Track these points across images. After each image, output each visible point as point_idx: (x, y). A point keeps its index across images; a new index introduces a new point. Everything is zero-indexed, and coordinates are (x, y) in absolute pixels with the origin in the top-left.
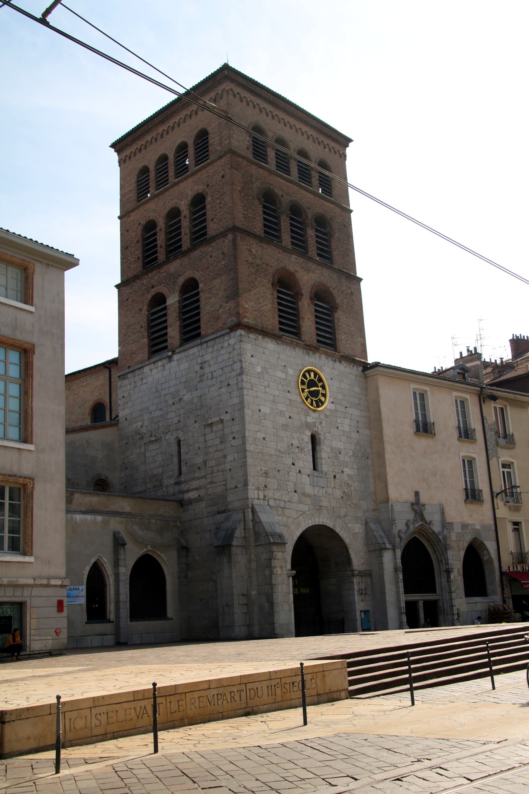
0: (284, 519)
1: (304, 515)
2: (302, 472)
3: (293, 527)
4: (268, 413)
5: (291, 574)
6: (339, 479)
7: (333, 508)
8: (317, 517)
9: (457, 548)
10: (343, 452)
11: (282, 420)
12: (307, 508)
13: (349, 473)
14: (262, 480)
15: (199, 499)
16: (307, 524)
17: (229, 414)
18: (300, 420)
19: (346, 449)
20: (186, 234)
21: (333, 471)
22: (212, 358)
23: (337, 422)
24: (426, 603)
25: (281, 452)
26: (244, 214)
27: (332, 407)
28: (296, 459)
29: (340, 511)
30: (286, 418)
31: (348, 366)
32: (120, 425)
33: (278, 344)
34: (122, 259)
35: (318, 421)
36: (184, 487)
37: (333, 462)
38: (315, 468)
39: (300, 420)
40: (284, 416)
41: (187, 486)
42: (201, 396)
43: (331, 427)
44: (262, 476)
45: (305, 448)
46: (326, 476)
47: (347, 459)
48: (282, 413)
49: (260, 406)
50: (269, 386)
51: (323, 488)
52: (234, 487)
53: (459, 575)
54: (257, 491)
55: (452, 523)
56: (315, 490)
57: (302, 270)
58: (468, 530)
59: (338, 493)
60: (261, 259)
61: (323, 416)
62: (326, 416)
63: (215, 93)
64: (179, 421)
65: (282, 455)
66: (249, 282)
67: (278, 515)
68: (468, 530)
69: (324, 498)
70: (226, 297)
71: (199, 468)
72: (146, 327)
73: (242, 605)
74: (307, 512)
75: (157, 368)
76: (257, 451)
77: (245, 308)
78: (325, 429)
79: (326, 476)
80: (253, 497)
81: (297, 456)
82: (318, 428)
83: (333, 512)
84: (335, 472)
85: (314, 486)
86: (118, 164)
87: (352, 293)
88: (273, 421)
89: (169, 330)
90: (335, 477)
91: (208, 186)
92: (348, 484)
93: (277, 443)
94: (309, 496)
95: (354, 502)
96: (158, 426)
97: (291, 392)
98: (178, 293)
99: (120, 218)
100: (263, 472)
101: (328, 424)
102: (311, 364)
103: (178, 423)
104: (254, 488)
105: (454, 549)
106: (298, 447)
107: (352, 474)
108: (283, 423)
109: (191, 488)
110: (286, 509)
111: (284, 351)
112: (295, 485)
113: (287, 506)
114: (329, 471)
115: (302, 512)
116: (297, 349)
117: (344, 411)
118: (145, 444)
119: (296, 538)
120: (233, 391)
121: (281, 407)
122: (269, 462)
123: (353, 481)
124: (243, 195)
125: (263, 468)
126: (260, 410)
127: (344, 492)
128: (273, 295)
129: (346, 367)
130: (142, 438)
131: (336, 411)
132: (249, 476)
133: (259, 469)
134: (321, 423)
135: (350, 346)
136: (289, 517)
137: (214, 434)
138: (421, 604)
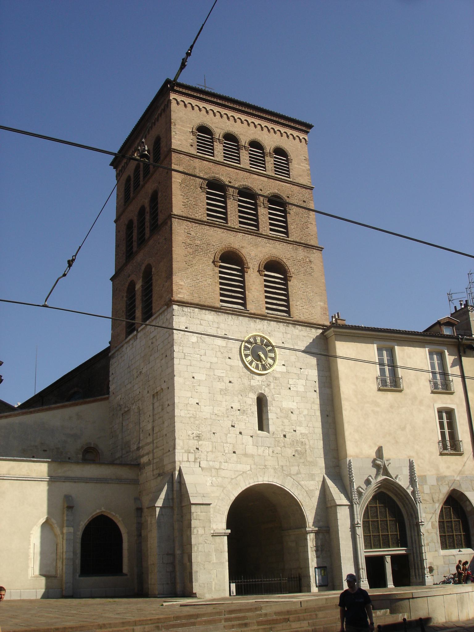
0: (218, 480)
1: (245, 475)
2: (242, 433)
4: (204, 379)
5: (225, 533)
6: (290, 439)
7: (282, 466)
8: (261, 476)
10: (296, 412)
11: (220, 386)
12: (248, 467)
13: (303, 432)
14: (193, 444)
15: (149, 463)
16: (247, 483)
17: (166, 383)
18: (242, 384)
19: (299, 409)
20: (147, 227)
21: (282, 431)
22: (158, 333)
23: (289, 384)
24: (393, 557)
26: (183, 202)
27: (284, 369)
28: (237, 421)
29: (290, 469)
30: (225, 383)
31: (303, 329)
32: (111, 399)
33: (218, 314)
34: (116, 255)
35: (265, 383)
36: (142, 452)
37: (283, 422)
38: (261, 428)
39: (242, 384)
40: (223, 381)
41: (143, 451)
42: (151, 368)
43: (282, 389)
44: (194, 440)
45: (247, 411)
46: (274, 436)
48: (220, 379)
49: (193, 374)
50: (205, 354)
51: (269, 447)
52: (168, 451)
53: (432, 528)
54: (187, 454)
55: (425, 476)
56: (259, 451)
57: (250, 246)
58: (445, 482)
59: (290, 452)
60: (201, 240)
61: (272, 378)
62: (276, 378)
63: (164, 105)
64: (140, 392)
65: (219, 418)
66: (185, 261)
67: (211, 476)
68: (445, 482)
69: (270, 458)
70: (166, 277)
71: (149, 435)
72: (125, 311)
73: (167, 564)
74: (248, 472)
75: (129, 346)
76: (188, 416)
77: (180, 285)
78: (273, 391)
79: (274, 436)
80: (181, 460)
81: (237, 419)
82: (265, 390)
83: (282, 471)
84: (285, 432)
85: (257, 446)
86: (116, 178)
87: (310, 261)
88: (208, 387)
89: (137, 311)
90: (285, 436)
91: (159, 183)
92: (302, 442)
93: (214, 407)
94: (252, 456)
96: (129, 398)
97: (231, 358)
98: (141, 278)
99: (116, 221)
100: (194, 435)
101: (277, 386)
102: (258, 331)
103: (139, 394)
104: (183, 451)
105: (428, 501)
106: (239, 410)
107: (307, 432)
108: (221, 388)
109: (145, 453)
110: (221, 470)
111: (225, 321)
112: (234, 446)
113: (223, 467)
114: (277, 431)
115: (242, 472)
117: (299, 373)
118: (122, 414)
119: (233, 498)
120: (169, 362)
121: (218, 373)
122: (203, 425)
123: (308, 439)
124: (184, 185)
125: (195, 432)
126: (193, 378)
127: (296, 451)
128: (214, 270)
129: (302, 330)
130: (120, 410)
131: (288, 372)
132: (177, 440)
133: (190, 432)
134: (268, 385)
135: (307, 311)
136: (225, 477)
137: (158, 401)
138: (388, 559)
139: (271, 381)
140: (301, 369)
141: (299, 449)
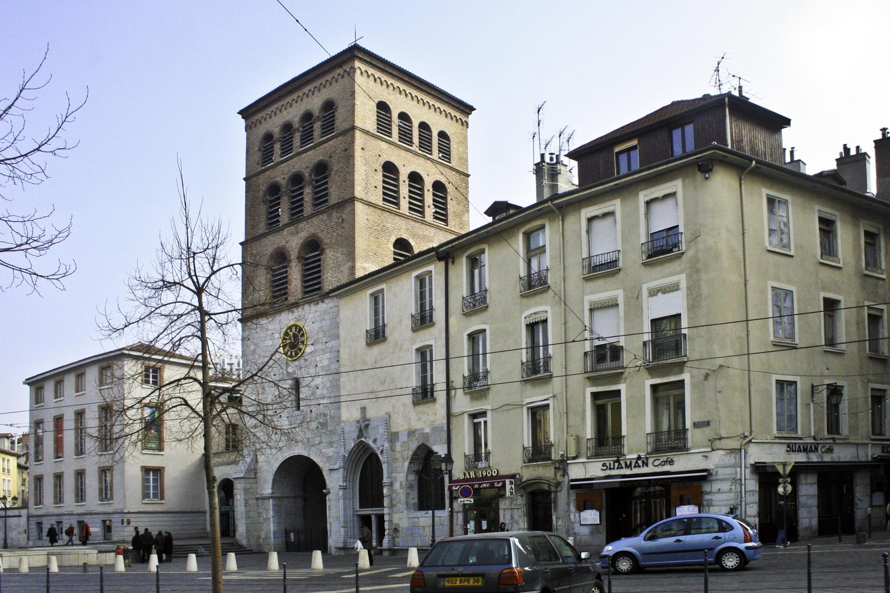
3: (272, 461)
7: (308, 439)
9: (401, 460)
23: (316, 361)
47: (325, 392)
53: (401, 488)
95: (330, 428)
127: (320, 423)
135: (336, 279)
141: (321, 421)
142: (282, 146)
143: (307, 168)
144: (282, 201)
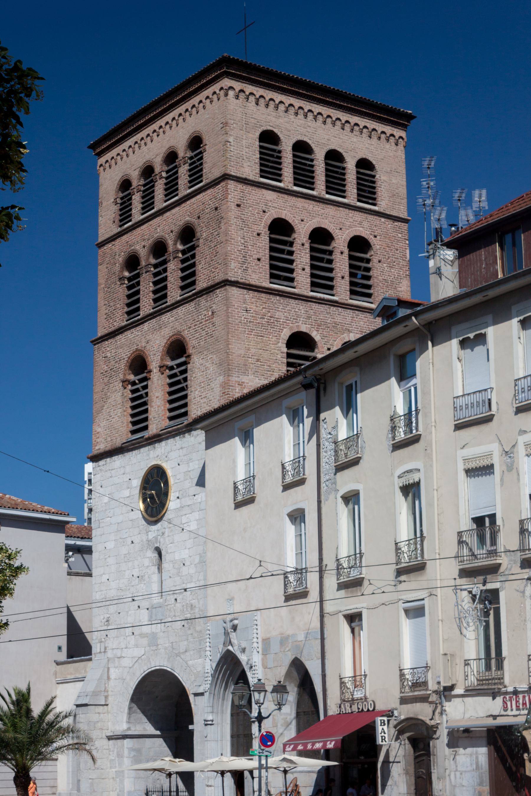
1: (140, 661)
11: (124, 550)
25: (122, 590)
45: (145, 575)
55: (269, 638)
79: (166, 604)
82: (160, 542)
100: (105, 620)
106: (138, 577)
116: (142, 450)
133: (102, 617)
135: (205, 400)
139: (165, 526)
140: (195, 495)
142: (143, 197)
143: (172, 232)
144: (141, 279)
